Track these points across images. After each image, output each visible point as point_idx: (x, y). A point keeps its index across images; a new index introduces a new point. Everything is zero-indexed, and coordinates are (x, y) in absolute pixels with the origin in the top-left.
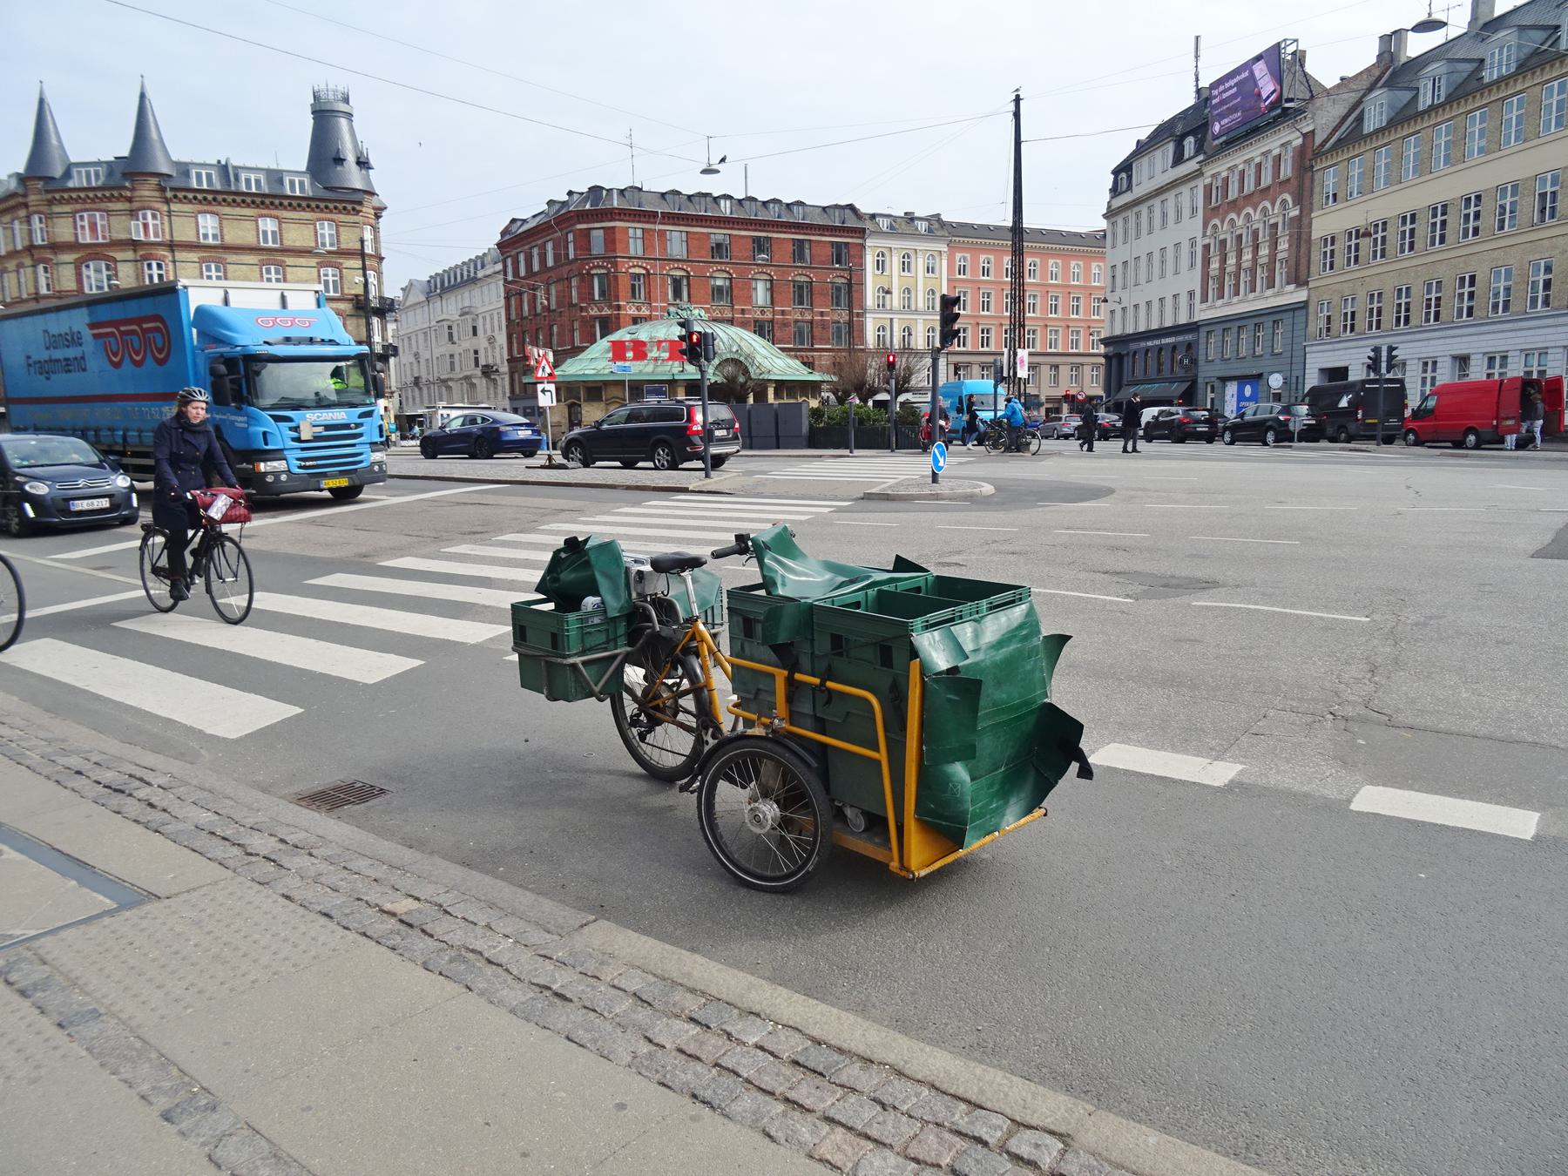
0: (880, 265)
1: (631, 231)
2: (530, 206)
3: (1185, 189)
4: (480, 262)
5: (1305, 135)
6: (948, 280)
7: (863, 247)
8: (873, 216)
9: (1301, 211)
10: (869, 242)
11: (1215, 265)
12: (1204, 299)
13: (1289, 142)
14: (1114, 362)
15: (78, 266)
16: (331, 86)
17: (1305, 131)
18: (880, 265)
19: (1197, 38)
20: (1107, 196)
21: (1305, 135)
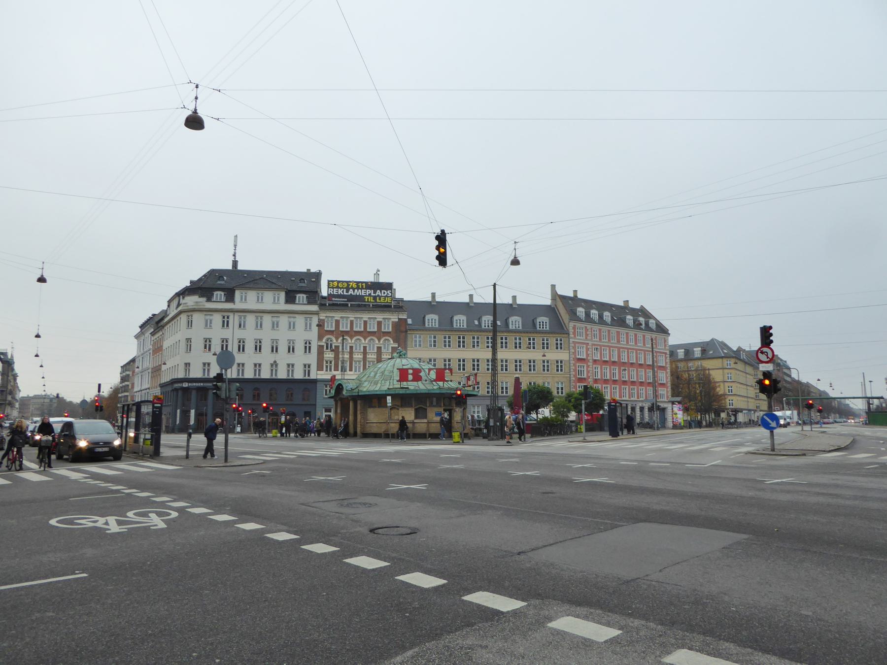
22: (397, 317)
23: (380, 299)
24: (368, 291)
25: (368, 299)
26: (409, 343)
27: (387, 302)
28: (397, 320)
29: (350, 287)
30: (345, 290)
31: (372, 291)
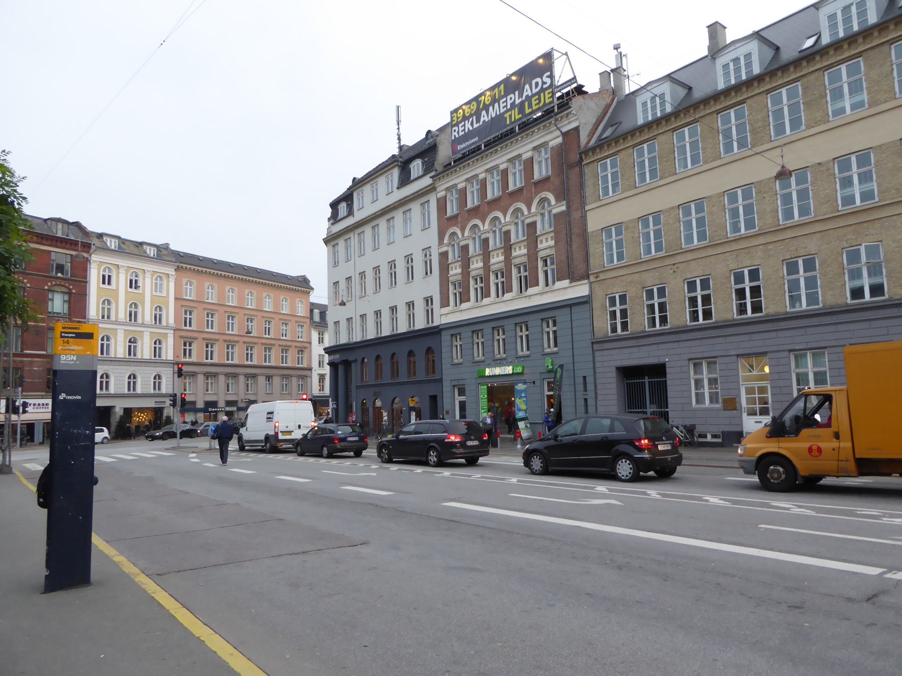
0: (106, 280)
3: (415, 207)
5: (565, 135)
6: (176, 299)
7: (87, 261)
8: (100, 236)
9: (568, 207)
10: (95, 258)
11: (455, 271)
12: (445, 303)
13: (545, 144)
14: (341, 369)
17: (564, 130)
18: (106, 280)
19: (398, 107)
20: (326, 224)
21: (565, 135)
22: (558, 133)
23: (530, 106)
24: (509, 97)
25: (510, 116)
26: (589, 191)
27: (545, 104)
28: (560, 140)
29: (481, 106)
30: (474, 117)
31: (517, 93)
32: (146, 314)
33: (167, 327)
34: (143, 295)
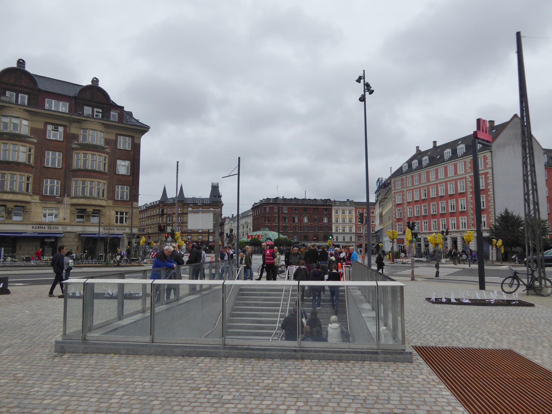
1: (275, 207)
2: (258, 201)
4: (249, 211)
10: (333, 208)
15: (167, 217)
16: (215, 182)
32: (347, 221)
33: (353, 223)
34: (346, 215)
